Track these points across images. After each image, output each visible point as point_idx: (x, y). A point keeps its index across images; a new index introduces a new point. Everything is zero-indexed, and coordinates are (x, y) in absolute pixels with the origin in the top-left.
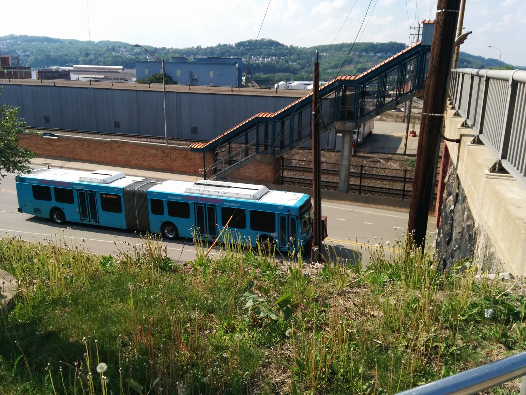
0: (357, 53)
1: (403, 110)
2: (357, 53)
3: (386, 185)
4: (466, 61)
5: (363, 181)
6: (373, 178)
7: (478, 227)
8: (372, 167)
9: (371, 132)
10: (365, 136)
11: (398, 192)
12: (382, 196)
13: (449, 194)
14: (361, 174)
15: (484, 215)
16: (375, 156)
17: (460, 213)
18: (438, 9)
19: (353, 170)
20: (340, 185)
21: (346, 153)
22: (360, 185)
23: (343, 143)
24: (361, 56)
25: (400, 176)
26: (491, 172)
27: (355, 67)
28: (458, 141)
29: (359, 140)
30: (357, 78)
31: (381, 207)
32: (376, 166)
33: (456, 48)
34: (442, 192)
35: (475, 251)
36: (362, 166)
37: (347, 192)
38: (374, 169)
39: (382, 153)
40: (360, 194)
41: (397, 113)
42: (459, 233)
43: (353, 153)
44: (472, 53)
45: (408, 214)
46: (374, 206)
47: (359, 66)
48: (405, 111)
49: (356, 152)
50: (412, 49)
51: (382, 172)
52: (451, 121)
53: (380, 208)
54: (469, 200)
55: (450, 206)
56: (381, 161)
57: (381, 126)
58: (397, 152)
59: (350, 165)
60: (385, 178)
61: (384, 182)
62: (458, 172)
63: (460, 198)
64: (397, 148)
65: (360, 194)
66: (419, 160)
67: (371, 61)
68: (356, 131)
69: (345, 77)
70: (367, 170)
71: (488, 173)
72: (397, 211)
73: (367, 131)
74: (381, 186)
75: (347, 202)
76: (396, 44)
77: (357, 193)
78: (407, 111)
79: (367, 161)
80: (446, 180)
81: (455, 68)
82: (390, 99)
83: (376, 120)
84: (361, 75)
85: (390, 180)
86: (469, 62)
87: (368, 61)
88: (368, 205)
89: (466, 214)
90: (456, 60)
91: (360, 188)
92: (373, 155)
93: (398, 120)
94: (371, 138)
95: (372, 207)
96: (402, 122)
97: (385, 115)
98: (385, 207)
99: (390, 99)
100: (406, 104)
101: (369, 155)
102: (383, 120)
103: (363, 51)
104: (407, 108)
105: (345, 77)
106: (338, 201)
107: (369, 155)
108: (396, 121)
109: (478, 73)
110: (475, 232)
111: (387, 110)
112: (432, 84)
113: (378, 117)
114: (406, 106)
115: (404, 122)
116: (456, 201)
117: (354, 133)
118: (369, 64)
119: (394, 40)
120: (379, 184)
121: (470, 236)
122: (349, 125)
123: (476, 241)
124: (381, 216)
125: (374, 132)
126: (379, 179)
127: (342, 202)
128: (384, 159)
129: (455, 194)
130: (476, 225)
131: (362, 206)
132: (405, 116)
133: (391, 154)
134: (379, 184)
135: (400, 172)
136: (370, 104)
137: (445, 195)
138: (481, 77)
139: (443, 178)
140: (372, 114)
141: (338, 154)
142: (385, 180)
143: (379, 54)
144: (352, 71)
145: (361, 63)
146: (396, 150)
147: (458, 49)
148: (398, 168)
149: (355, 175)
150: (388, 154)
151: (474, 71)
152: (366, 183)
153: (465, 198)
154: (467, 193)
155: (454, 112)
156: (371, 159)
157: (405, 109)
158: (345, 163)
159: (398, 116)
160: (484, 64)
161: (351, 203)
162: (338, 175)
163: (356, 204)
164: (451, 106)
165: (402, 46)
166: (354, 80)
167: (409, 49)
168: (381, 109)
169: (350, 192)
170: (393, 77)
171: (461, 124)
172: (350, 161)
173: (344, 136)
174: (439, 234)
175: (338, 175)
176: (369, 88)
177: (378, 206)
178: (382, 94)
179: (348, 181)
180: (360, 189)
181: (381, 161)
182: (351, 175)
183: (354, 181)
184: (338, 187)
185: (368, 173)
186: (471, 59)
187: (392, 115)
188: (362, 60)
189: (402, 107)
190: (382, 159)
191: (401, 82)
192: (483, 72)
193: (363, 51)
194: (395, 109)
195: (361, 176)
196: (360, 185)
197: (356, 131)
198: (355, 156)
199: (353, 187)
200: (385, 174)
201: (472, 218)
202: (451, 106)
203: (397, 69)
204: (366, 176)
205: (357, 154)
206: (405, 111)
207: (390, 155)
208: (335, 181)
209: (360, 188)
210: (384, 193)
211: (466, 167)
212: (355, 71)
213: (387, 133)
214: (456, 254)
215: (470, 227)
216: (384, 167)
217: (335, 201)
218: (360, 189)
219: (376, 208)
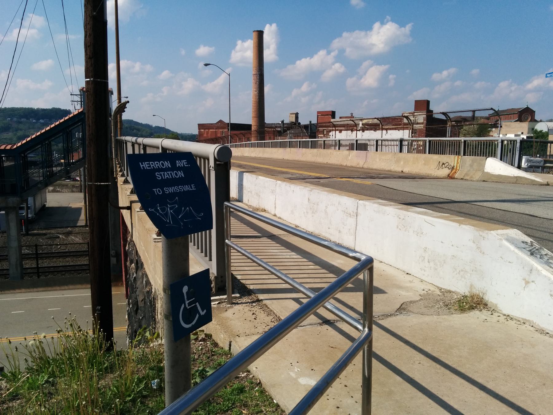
0: (15, 119)
1: (78, 178)
2: (15, 119)
3: (70, 261)
4: (136, 129)
5: (40, 262)
6: (54, 257)
7: (155, 292)
8: (50, 245)
9: (45, 205)
10: (37, 211)
11: (85, 268)
12: (67, 274)
13: (132, 262)
14: (37, 254)
15: (158, 279)
16: (53, 231)
17: (141, 280)
18: (86, 77)
19: (25, 251)
20: (11, 272)
21: (14, 232)
22: (38, 268)
23: (8, 222)
24: (20, 123)
25: (85, 249)
26: (158, 236)
27: (15, 134)
28: (129, 208)
29: (30, 216)
30: (15, 147)
31: (66, 287)
32: (55, 243)
33: (118, 116)
34: (126, 260)
35: (156, 317)
36: (36, 246)
37: (22, 278)
38: (53, 247)
39: (60, 228)
40: (39, 278)
41: (72, 183)
42: (142, 300)
43: (24, 232)
44: (140, 121)
45: (89, 290)
46: (58, 288)
47: (20, 133)
48: (81, 181)
49: (27, 230)
50: (74, 116)
51: (63, 249)
52: (122, 189)
53: (65, 290)
54: (145, 266)
55: (133, 274)
56: (61, 236)
57: (55, 199)
58: (78, 224)
59: (20, 247)
60: (68, 254)
61: (67, 259)
62: (134, 239)
63: (139, 265)
64: (78, 220)
65: (39, 278)
66: (92, 232)
67: (33, 128)
68: (24, 205)
69: (4, 146)
70: (45, 248)
71: (155, 237)
72: (85, 288)
73: (38, 205)
74: (63, 264)
75: (23, 290)
76: (59, 110)
77: (35, 277)
78: (82, 179)
79: (43, 239)
80: (127, 248)
81: (121, 136)
82: (59, 169)
83: (49, 192)
84: (19, 144)
85: (74, 256)
86: (138, 130)
87: (29, 128)
88: (50, 288)
89: (145, 280)
90: (121, 128)
91: (38, 270)
92: (49, 231)
93: (74, 189)
94: (45, 212)
95: (56, 290)
96: (79, 192)
97: (59, 185)
98: (71, 287)
99: (59, 169)
100: (80, 173)
101: (44, 232)
102: (58, 192)
103: (21, 117)
104: (82, 177)
105: (4, 146)
106: (12, 291)
107: (44, 232)
108: (73, 192)
109: (136, 141)
110: (153, 298)
111: (57, 181)
112: (92, 153)
113: (51, 188)
114: (80, 175)
115: (81, 192)
116: (137, 268)
117: (22, 208)
118: (32, 131)
119: (57, 106)
120: (60, 262)
121: (150, 301)
122: (12, 200)
123: (155, 306)
124: (67, 298)
125: (48, 205)
126: (60, 257)
127: (17, 291)
128: (64, 234)
129: (135, 262)
130: (153, 290)
131: (43, 291)
132: (81, 186)
133: (71, 227)
134: (60, 262)
135: (83, 245)
136: (36, 174)
137: (128, 263)
138: (139, 145)
139: (125, 246)
140: (39, 185)
141: (5, 235)
142: (67, 256)
143: (41, 121)
144: (11, 139)
145: (21, 130)
146: (77, 223)
147: (121, 117)
148: (81, 241)
149: (30, 256)
150: (68, 227)
151: (134, 139)
152: (45, 263)
153: (142, 264)
154: (143, 260)
155: (124, 178)
156: (48, 235)
157: (80, 178)
158: (14, 244)
159: (73, 186)
160: (153, 131)
161: (28, 290)
162: (7, 259)
163: (35, 290)
164: (121, 173)
165: (68, 112)
166: (10, 149)
167: (71, 116)
168: (50, 180)
169: (26, 278)
170: (57, 147)
171: (130, 190)
172: (19, 241)
173: (7, 214)
174: (129, 304)
175: (7, 259)
176: (32, 156)
177: (63, 288)
178: (48, 163)
179: (21, 265)
180: (38, 271)
181: (61, 236)
182: (23, 257)
183: (29, 264)
184: (9, 274)
185: (46, 252)
186: (140, 127)
187: (66, 186)
188: (21, 126)
189: (77, 176)
190: (60, 234)
191: (67, 152)
192: (140, 140)
193: (21, 117)
194: (69, 178)
195: (37, 257)
196: (38, 268)
197: (24, 205)
198: (27, 234)
199: (29, 271)
200: (67, 250)
201: (151, 285)
202: (121, 173)
203: (61, 137)
204: (44, 255)
205: (30, 232)
206: (81, 181)
207: (69, 229)
208: (5, 268)
209: (38, 270)
210: (68, 271)
211: (138, 233)
212: (15, 139)
213: (65, 205)
214: (143, 322)
215: (149, 292)
216: (65, 242)
217: (6, 292)
218: (38, 271)
219: (60, 290)
